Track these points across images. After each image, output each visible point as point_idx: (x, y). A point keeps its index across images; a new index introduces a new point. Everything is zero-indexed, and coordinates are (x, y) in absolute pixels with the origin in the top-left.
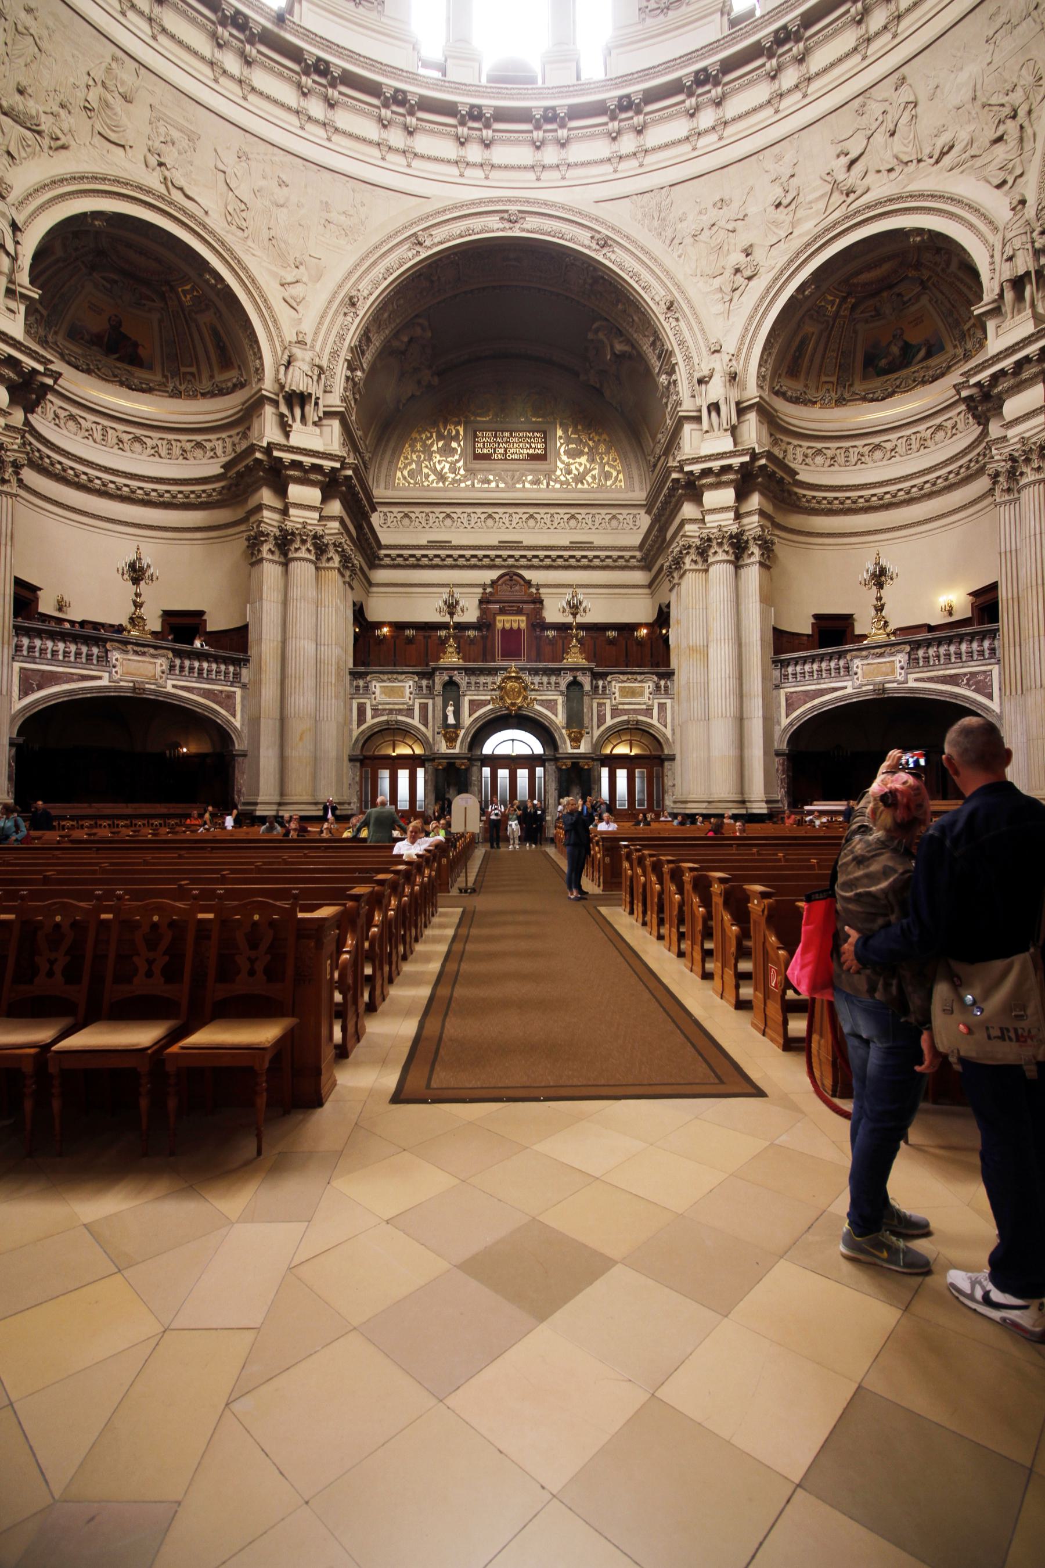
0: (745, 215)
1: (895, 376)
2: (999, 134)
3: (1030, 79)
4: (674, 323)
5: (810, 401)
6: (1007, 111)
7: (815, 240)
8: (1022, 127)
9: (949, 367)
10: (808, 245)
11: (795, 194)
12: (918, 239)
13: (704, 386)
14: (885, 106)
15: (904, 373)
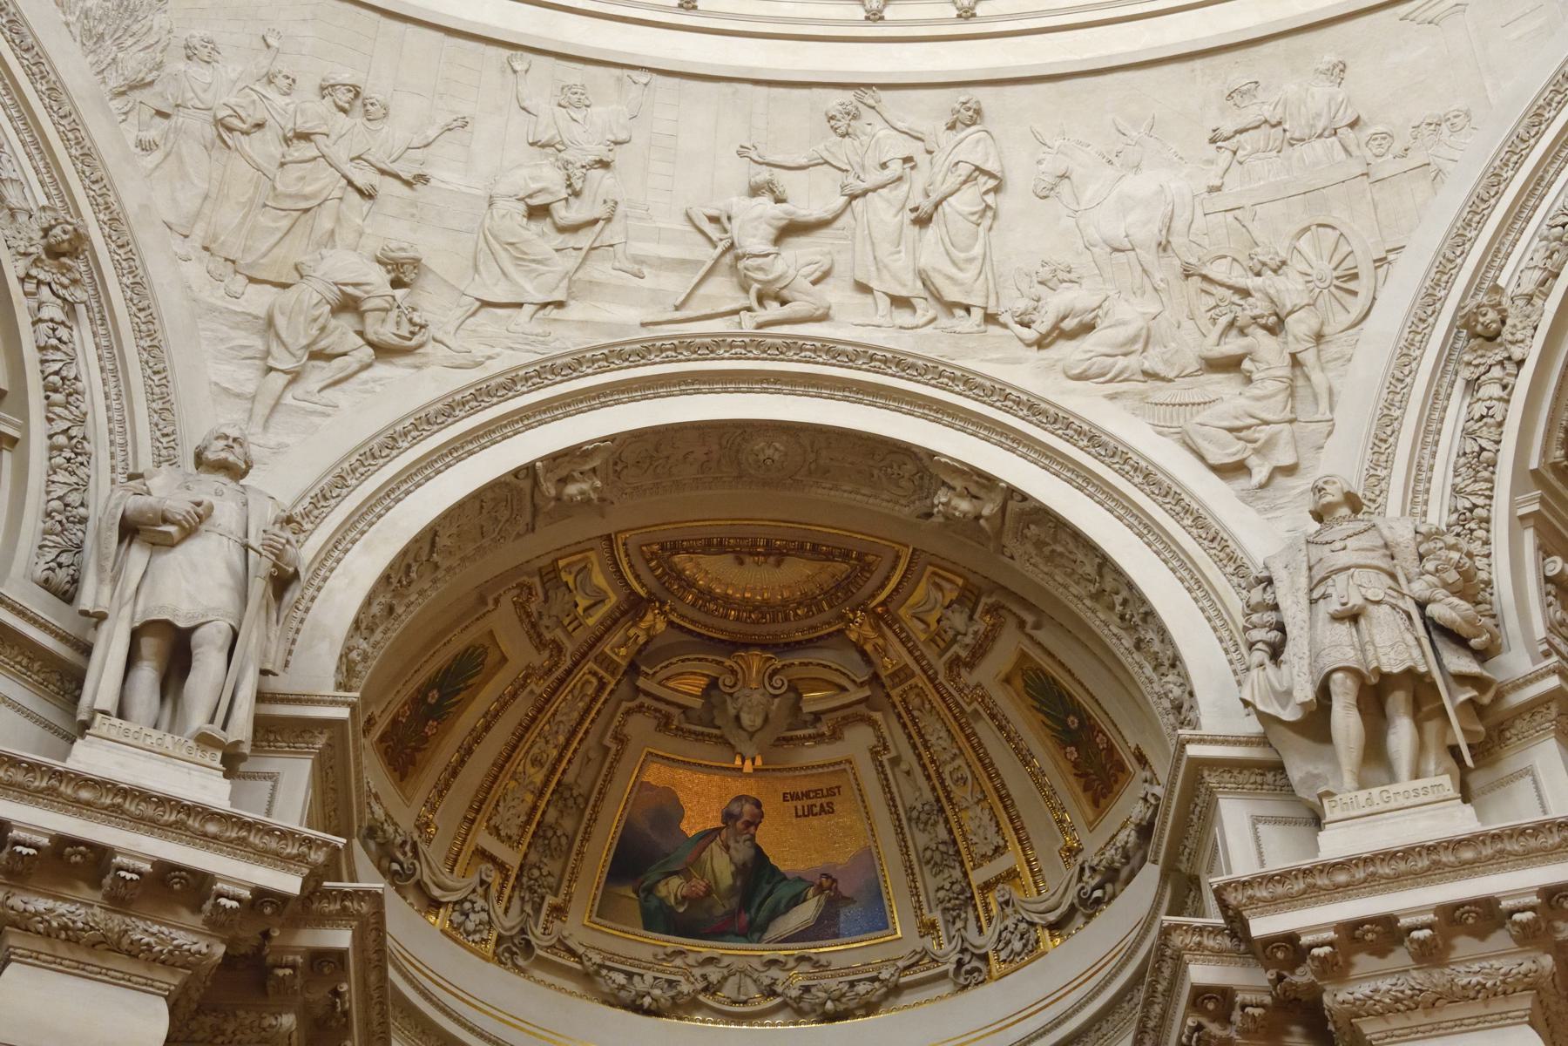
0: (423, 178)
1: (706, 948)
2: (1233, 345)
3: (1324, 268)
4: (53, 311)
5: (420, 887)
6: (1258, 306)
7: (644, 352)
8: (1295, 361)
9: (895, 990)
10: (615, 355)
11: (600, 211)
12: (964, 505)
13: (138, 557)
14: (914, 149)
15: (733, 951)
